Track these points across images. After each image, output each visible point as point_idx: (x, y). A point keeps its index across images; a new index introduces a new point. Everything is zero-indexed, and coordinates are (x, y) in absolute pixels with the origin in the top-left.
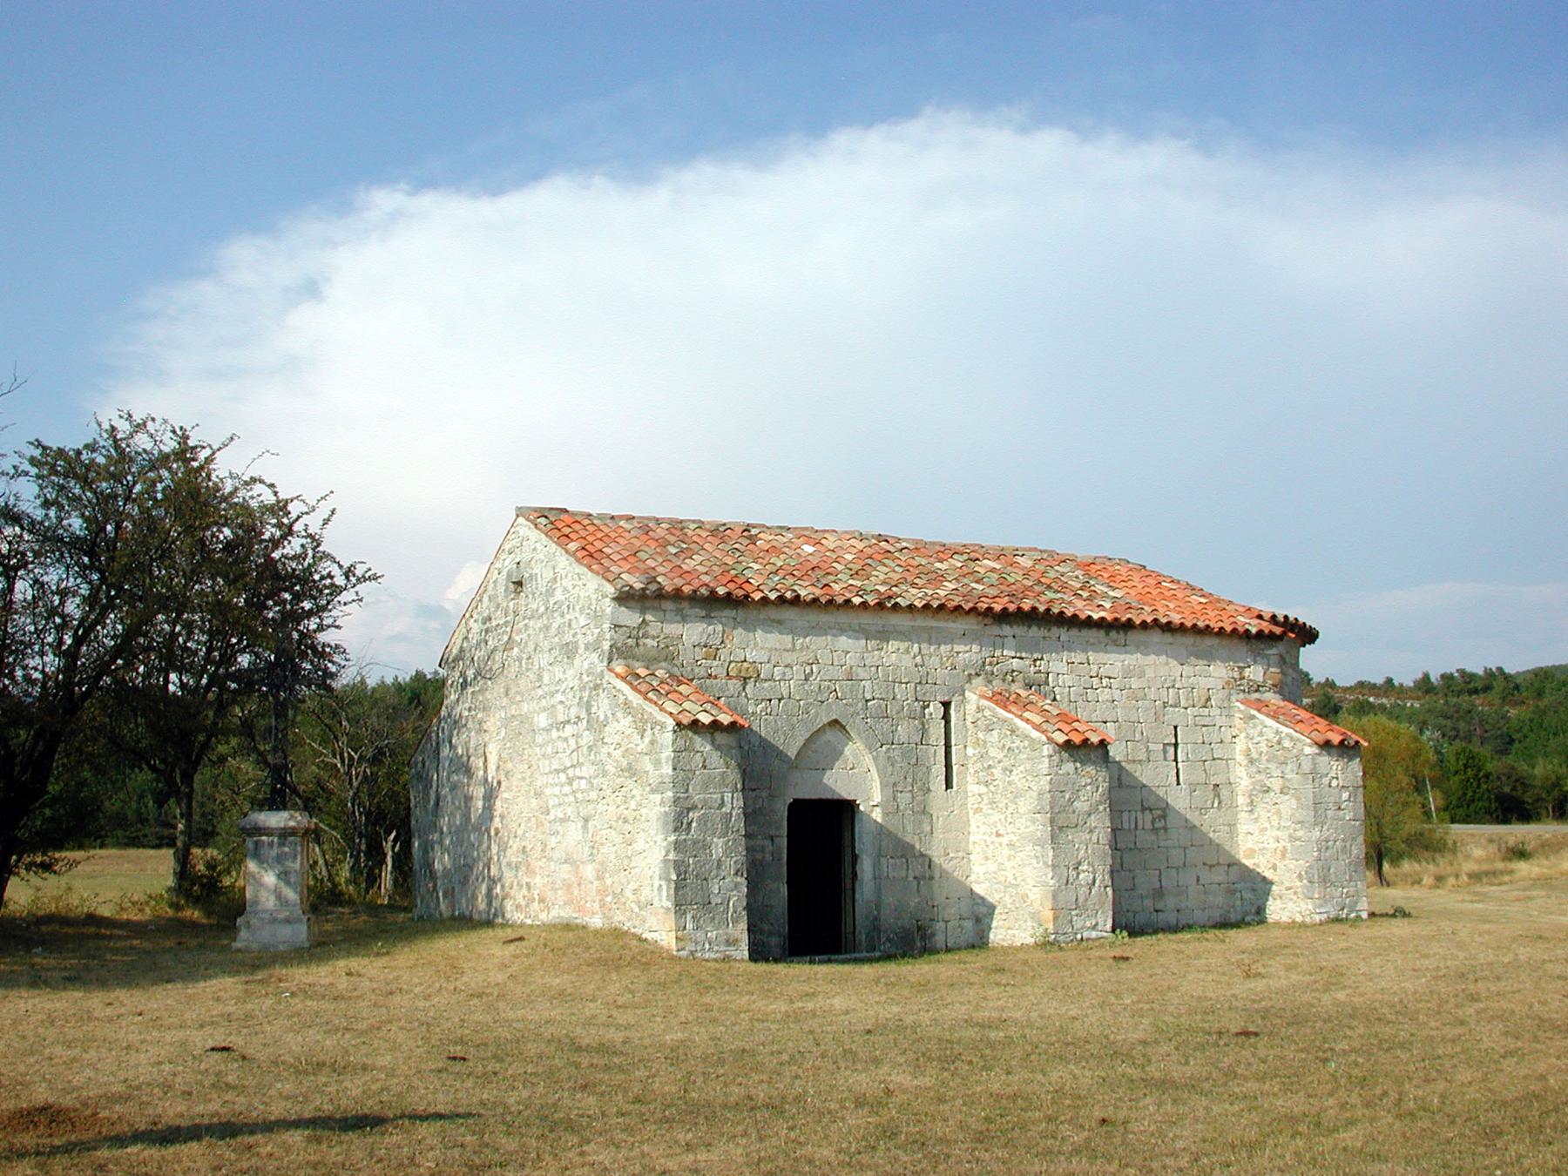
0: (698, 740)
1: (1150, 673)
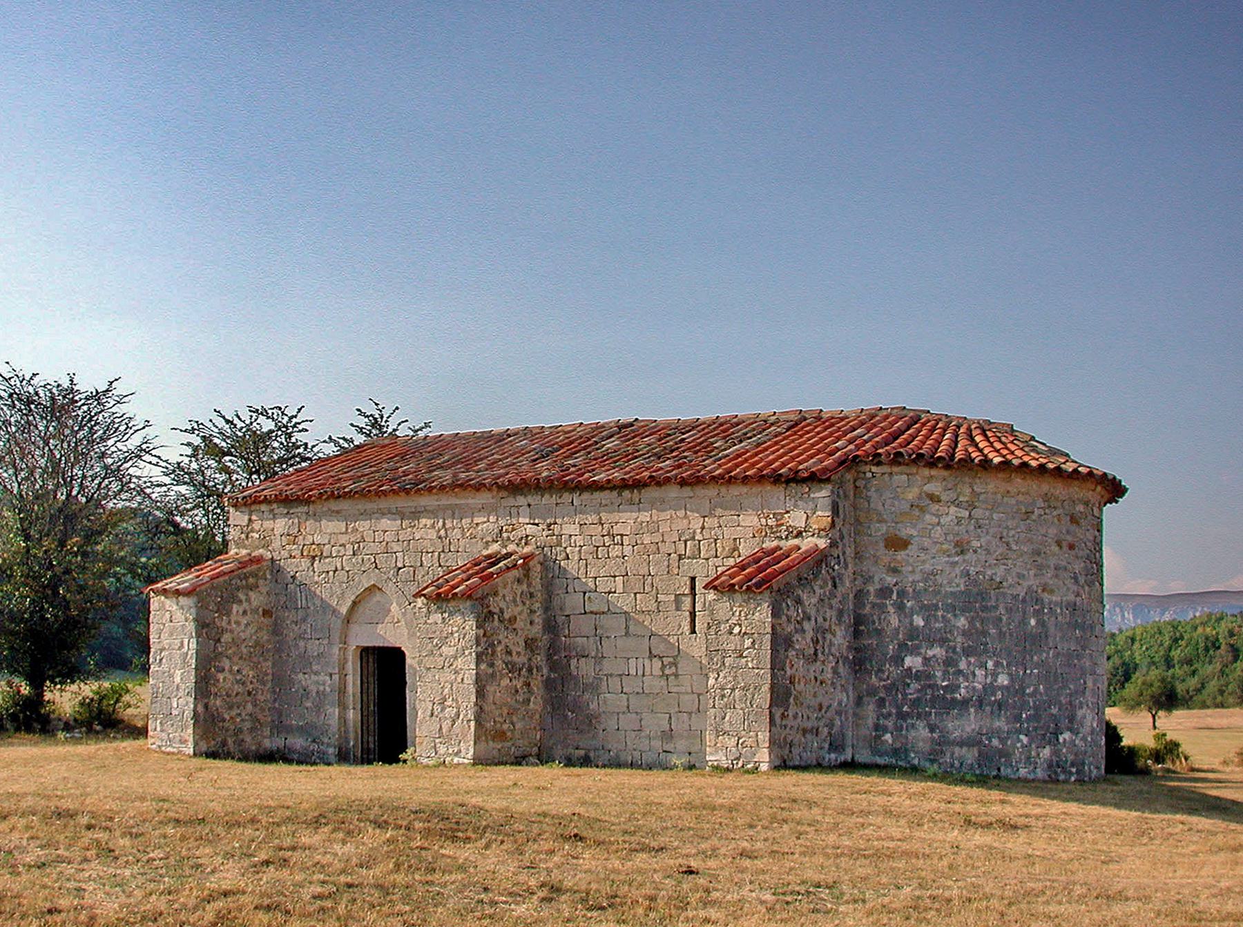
0: (168, 602)
1: (664, 528)
